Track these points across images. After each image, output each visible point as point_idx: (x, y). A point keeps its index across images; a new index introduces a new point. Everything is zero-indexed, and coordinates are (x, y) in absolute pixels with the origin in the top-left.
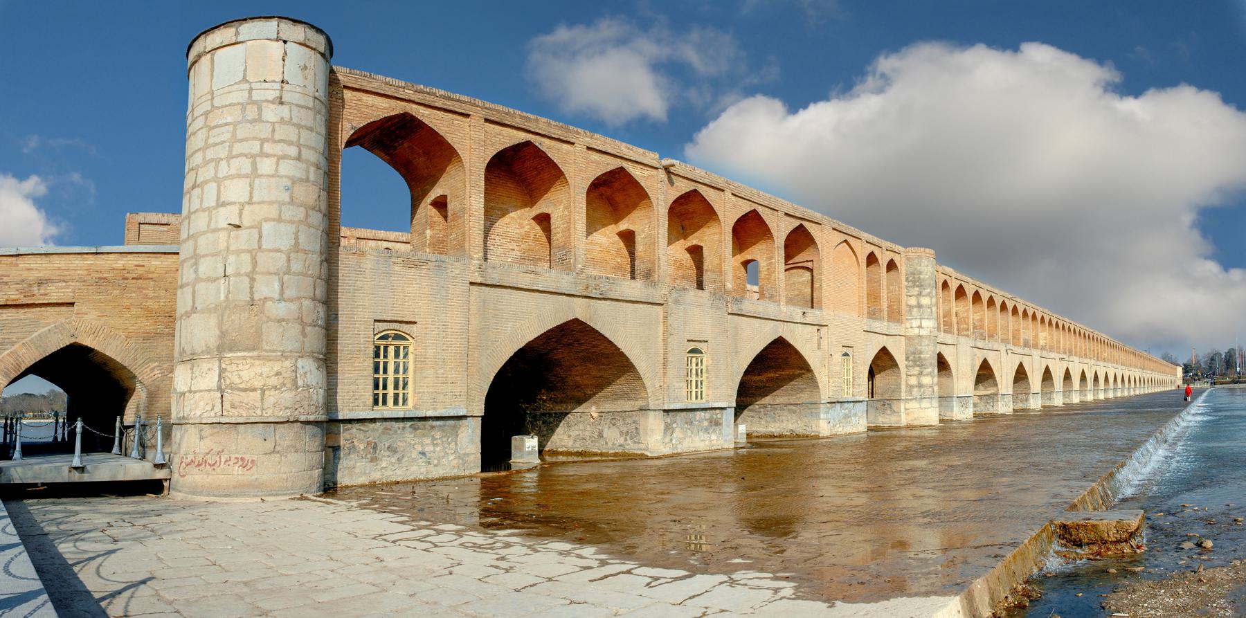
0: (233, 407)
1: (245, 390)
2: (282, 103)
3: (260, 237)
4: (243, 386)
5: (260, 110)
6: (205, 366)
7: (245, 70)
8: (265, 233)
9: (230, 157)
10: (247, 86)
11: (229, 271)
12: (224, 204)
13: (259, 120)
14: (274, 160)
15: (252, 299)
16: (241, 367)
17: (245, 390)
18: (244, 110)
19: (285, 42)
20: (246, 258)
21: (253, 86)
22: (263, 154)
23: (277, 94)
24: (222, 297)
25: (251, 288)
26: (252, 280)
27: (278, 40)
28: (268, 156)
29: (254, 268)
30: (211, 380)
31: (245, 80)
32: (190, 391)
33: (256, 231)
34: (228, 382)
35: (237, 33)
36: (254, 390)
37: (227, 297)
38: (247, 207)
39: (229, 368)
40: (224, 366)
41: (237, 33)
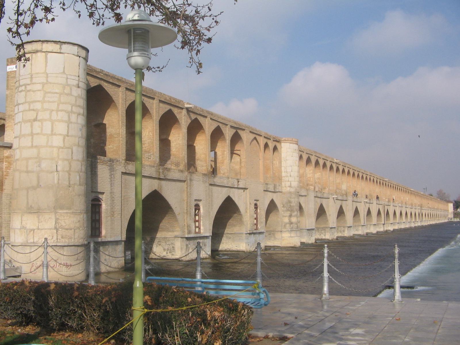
0: (62, 237)
1: (67, 229)
2: (79, 87)
3: (72, 153)
4: (66, 227)
5: (71, 89)
6: (47, 216)
7: (64, 68)
8: (74, 151)
9: (58, 111)
10: (65, 76)
11: (59, 168)
12: (55, 134)
13: (70, 94)
14: (76, 115)
15: (69, 183)
16: (65, 218)
17: (67, 229)
18: (64, 88)
19: (80, 57)
20: (66, 163)
21: (69, 77)
22: (72, 112)
23: (77, 82)
24: (56, 181)
25: (69, 178)
26: (70, 174)
27: (77, 56)
28: (74, 113)
29: (70, 169)
30: (51, 224)
31: (64, 72)
32: (38, 229)
33: (70, 150)
34: (60, 225)
35: (60, 48)
36: (71, 229)
37: (58, 183)
38: (66, 137)
39: (60, 218)
40: (57, 217)
41: (60, 48)
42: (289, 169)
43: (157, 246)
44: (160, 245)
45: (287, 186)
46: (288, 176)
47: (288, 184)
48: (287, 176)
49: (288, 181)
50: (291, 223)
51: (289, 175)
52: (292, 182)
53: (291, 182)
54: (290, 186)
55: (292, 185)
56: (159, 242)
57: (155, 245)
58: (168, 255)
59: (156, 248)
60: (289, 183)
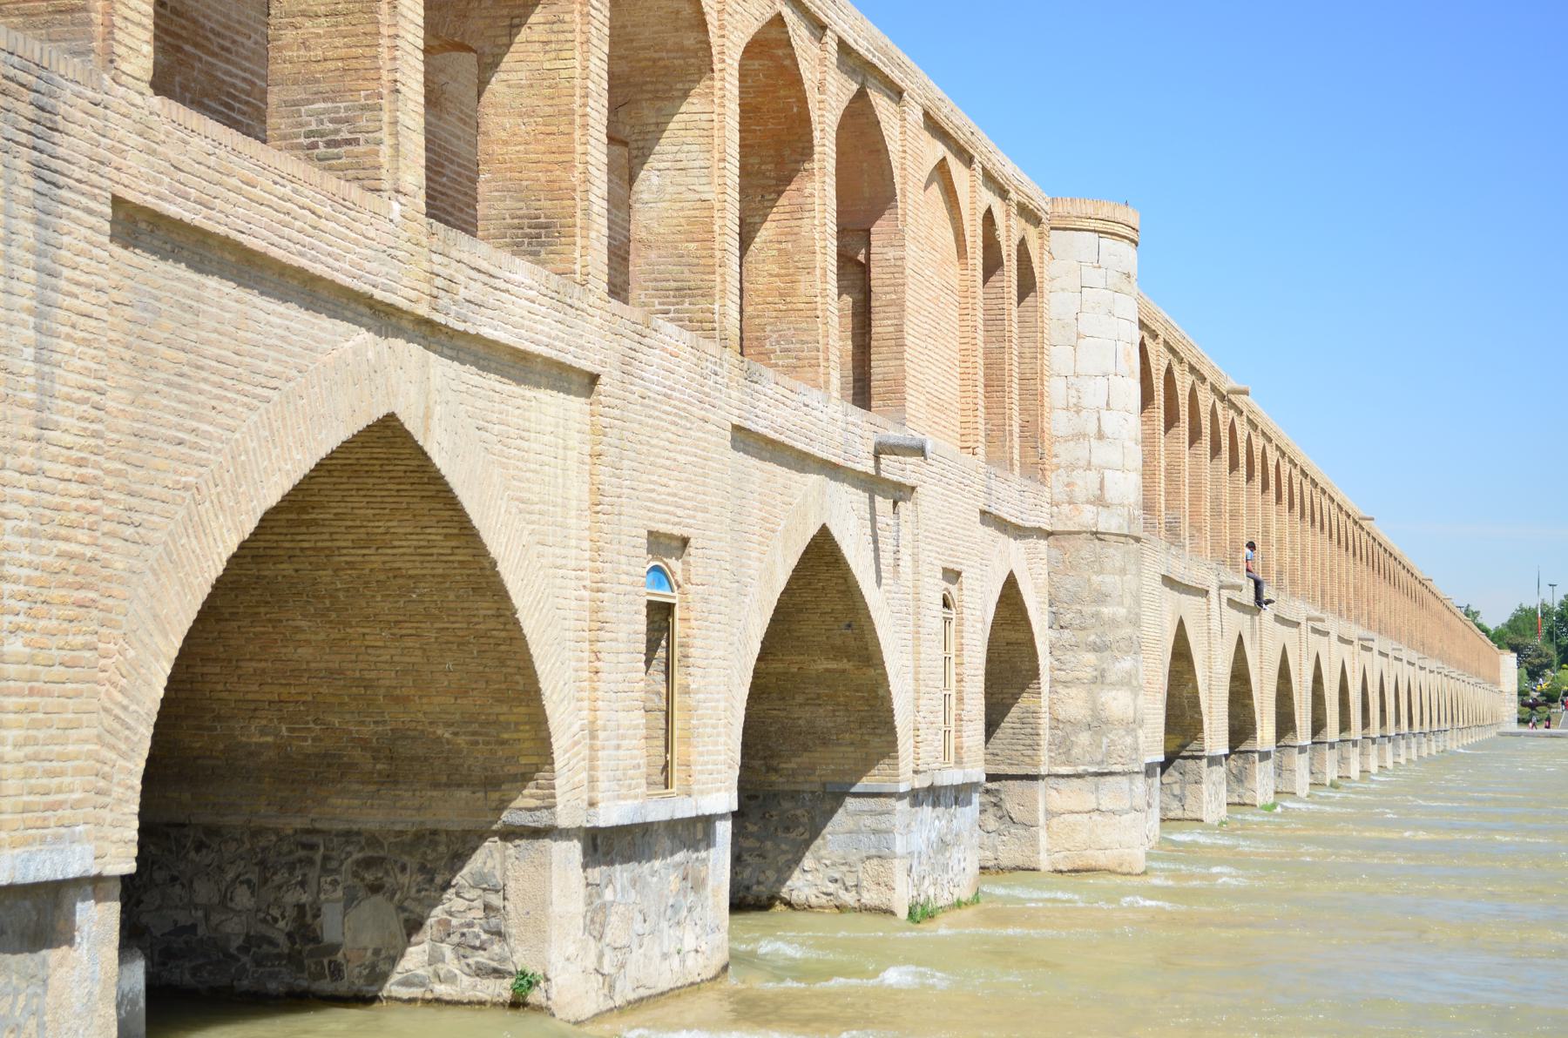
42: (1094, 393)
43: (351, 900)
44: (375, 888)
45: (1080, 493)
46: (1084, 436)
47: (1086, 483)
48: (1080, 436)
49: (1089, 467)
50: (1098, 724)
51: (1092, 428)
52: (1108, 474)
53: (1101, 469)
54: (1100, 501)
55: (1110, 495)
56: (368, 863)
57: (339, 893)
58: (442, 969)
59: (346, 907)
60: (1093, 476)
